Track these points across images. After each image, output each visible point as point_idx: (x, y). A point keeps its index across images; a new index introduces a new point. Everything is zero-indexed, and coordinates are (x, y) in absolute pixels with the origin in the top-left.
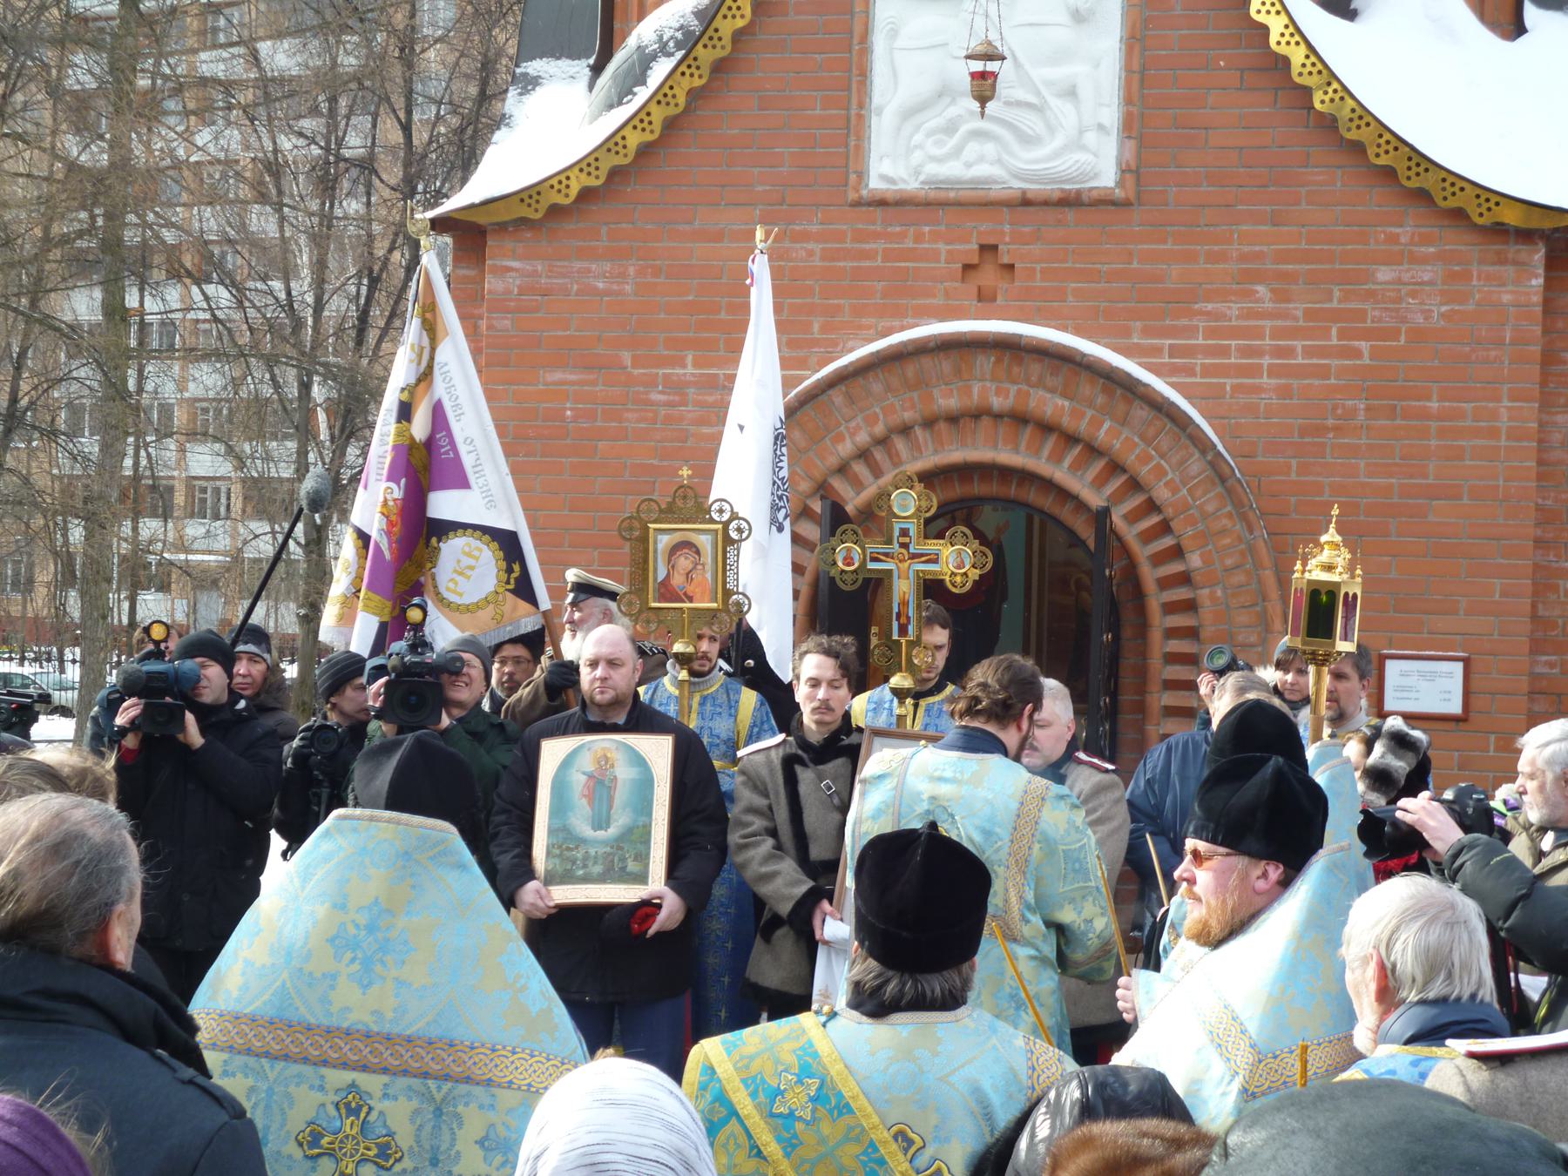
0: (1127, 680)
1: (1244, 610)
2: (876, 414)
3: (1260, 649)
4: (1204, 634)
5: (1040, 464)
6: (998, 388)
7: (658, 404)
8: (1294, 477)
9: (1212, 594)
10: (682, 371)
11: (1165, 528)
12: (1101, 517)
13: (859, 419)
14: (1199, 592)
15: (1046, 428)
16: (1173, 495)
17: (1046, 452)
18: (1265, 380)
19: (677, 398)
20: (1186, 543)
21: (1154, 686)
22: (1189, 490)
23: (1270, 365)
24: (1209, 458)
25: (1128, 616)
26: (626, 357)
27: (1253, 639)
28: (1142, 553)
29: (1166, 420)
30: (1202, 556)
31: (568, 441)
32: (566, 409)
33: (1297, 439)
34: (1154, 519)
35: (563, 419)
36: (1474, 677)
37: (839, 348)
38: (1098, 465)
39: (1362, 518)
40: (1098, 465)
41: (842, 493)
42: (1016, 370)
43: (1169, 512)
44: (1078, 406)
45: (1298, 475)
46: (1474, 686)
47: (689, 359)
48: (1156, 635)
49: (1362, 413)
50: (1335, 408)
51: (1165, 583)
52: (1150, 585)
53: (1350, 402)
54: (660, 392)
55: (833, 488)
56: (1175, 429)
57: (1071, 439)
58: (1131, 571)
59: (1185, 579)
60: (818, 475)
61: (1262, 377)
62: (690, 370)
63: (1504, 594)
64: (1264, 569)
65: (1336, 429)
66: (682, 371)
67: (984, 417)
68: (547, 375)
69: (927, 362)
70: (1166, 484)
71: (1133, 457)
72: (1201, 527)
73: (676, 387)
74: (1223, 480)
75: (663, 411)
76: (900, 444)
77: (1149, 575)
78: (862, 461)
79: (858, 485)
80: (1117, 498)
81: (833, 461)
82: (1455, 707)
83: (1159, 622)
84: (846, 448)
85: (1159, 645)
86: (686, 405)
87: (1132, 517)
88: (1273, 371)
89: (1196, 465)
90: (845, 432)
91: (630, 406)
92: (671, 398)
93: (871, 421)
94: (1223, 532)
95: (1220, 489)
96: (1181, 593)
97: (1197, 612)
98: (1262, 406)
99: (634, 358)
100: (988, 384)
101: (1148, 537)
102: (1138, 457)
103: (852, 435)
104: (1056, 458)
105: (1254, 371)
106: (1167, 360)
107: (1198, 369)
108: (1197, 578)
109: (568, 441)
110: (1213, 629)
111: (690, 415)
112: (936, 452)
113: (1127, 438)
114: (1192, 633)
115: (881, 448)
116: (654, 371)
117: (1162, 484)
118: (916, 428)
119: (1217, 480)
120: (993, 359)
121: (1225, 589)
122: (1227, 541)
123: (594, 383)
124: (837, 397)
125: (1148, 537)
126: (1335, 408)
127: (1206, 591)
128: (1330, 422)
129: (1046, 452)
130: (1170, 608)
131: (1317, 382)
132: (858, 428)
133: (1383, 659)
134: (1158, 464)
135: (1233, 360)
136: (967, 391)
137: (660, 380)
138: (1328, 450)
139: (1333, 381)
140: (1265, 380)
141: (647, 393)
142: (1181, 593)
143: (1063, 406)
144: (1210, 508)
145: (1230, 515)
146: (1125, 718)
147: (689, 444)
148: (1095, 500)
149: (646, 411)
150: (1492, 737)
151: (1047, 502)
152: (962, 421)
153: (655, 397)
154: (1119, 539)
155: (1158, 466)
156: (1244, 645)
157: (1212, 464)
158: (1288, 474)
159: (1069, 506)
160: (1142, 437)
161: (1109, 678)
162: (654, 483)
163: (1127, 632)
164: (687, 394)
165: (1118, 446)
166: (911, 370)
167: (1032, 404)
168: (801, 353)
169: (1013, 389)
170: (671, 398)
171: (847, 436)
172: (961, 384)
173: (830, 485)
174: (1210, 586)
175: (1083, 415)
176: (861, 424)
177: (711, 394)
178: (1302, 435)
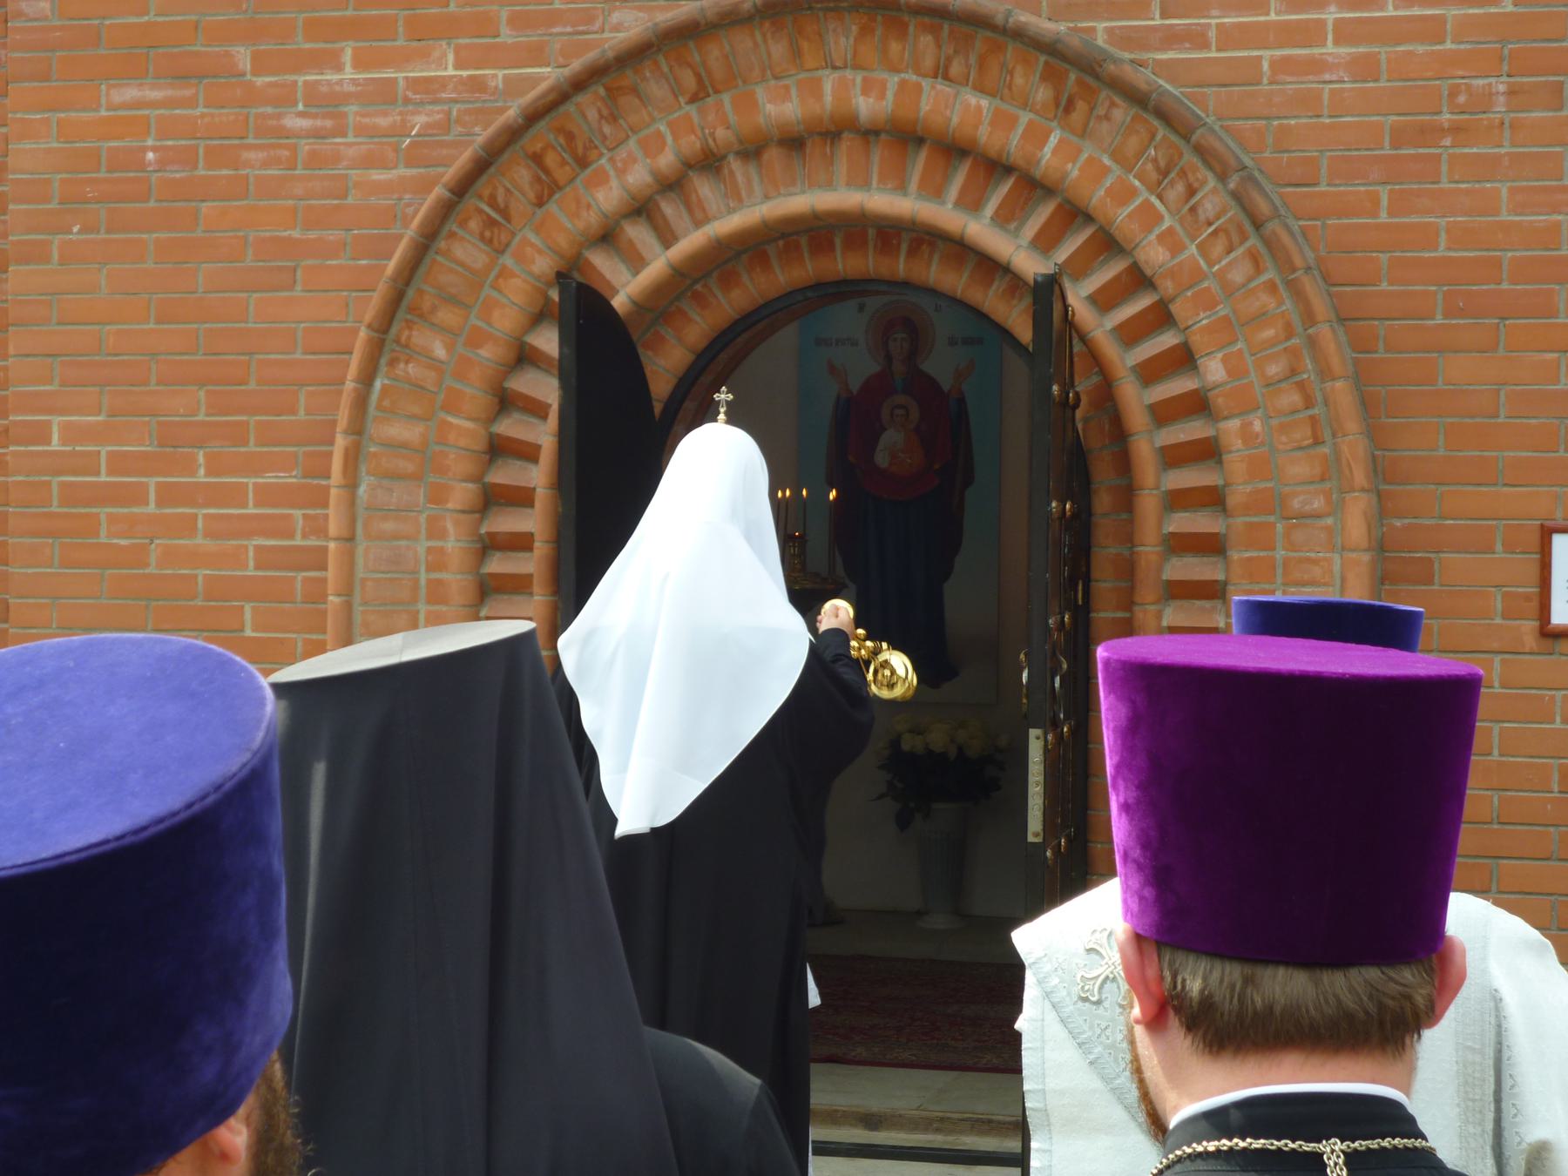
0: (1104, 583)
1: (1299, 454)
2: (659, 135)
3: (1329, 521)
4: (1232, 500)
5: (945, 214)
6: (865, 79)
7: (299, 134)
8: (1383, 217)
9: (1246, 428)
10: (335, 77)
11: (1161, 317)
12: (1046, 292)
13: (632, 144)
14: (1223, 425)
15: (953, 150)
16: (1173, 256)
17: (953, 191)
18: (1330, 48)
19: (328, 123)
20: (1197, 341)
21: (1147, 593)
22: (1199, 247)
23: (1337, 22)
24: (1232, 186)
25: (1103, 477)
26: (243, 56)
27: (1318, 504)
28: (1124, 361)
29: (1156, 123)
30: (1225, 360)
31: (152, 204)
32: (144, 150)
33: (1388, 151)
34: (1142, 302)
35: (142, 166)
37: (597, 25)
38: (1043, 213)
39: (1505, 286)
40: (1043, 213)
41: (608, 276)
42: (895, 47)
43: (1168, 286)
44: (1005, 107)
45: (1391, 214)
47: (347, 56)
48: (1148, 503)
49: (1502, 99)
50: (1454, 93)
51: (1164, 414)
53: (1481, 82)
54: (301, 115)
55: (594, 268)
56: (1173, 138)
57: (994, 167)
58: (1106, 395)
59: (1197, 404)
60: (563, 242)
61: (1324, 45)
62: (349, 73)
65: (1456, 129)
66: (335, 77)
67: (845, 135)
68: (113, 92)
69: (742, 42)
70: (1160, 238)
71: (1102, 192)
72: (1223, 310)
73: (326, 102)
74: (1258, 225)
75: (305, 146)
76: (704, 189)
77: (1135, 399)
78: (642, 220)
79: (636, 262)
80: (1079, 266)
81: (591, 220)
83: (1155, 481)
84: (608, 197)
86: (344, 135)
87: (1104, 301)
88: (1344, 33)
89: (1212, 199)
90: (608, 167)
91: (250, 141)
92: (319, 123)
93: (652, 146)
94: (1260, 319)
95: (1253, 241)
96: (1190, 430)
97: (1220, 462)
98: (1326, 96)
99: (256, 57)
100: (849, 73)
101: (1131, 334)
102: (1109, 191)
103: (621, 172)
104: (971, 202)
105: (1310, 35)
106: (1158, 22)
107: (1212, 34)
108: (1219, 401)
109: (152, 204)
110: (1249, 488)
111: (351, 152)
112: (767, 197)
113: (1091, 160)
114: (1213, 499)
115: (673, 195)
116: (290, 78)
117: (1153, 237)
118: (731, 158)
119: (1248, 227)
120: (854, 28)
122: (1269, 333)
123: (191, 103)
124: (588, 106)
125: (1131, 334)
126: (1454, 93)
127: (1234, 424)
128: (1446, 117)
129: (953, 191)
130: (1174, 457)
131: (1421, 49)
132: (632, 159)
134: (1147, 203)
135: (1273, 17)
136: (814, 88)
137: (299, 95)
138: (1444, 168)
139: (1449, 45)
140: (1330, 48)
141: (279, 116)
142: (1190, 430)
143: (979, 108)
144: (1237, 276)
145: (1272, 287)
147: (350, 200)
148: (1031, 265)
149: (280, 146)
151: (956, 282)
152: (809, 144)
153: (293, 122)
154: (1083, 338)
155: (1147, 206)
157: (1236, 196)
158: (1375, 215)
159: (999, 285)
160: (1116, 156)
161: (1072, 582)
163: (1103, 502)
164: (344, 115)
165: (1075, 173)
166: (714, 54)
167: (925, 106)
168: (533, 37)
169: (893, 81)
170: (319, 123)
171: (612, 173)
172: (803, 75)
173: (588, 263)
174: (1240, 414)
175: (1014, 121)
176: (639, 154)
177: (385, 114)
178: (1395, 145)
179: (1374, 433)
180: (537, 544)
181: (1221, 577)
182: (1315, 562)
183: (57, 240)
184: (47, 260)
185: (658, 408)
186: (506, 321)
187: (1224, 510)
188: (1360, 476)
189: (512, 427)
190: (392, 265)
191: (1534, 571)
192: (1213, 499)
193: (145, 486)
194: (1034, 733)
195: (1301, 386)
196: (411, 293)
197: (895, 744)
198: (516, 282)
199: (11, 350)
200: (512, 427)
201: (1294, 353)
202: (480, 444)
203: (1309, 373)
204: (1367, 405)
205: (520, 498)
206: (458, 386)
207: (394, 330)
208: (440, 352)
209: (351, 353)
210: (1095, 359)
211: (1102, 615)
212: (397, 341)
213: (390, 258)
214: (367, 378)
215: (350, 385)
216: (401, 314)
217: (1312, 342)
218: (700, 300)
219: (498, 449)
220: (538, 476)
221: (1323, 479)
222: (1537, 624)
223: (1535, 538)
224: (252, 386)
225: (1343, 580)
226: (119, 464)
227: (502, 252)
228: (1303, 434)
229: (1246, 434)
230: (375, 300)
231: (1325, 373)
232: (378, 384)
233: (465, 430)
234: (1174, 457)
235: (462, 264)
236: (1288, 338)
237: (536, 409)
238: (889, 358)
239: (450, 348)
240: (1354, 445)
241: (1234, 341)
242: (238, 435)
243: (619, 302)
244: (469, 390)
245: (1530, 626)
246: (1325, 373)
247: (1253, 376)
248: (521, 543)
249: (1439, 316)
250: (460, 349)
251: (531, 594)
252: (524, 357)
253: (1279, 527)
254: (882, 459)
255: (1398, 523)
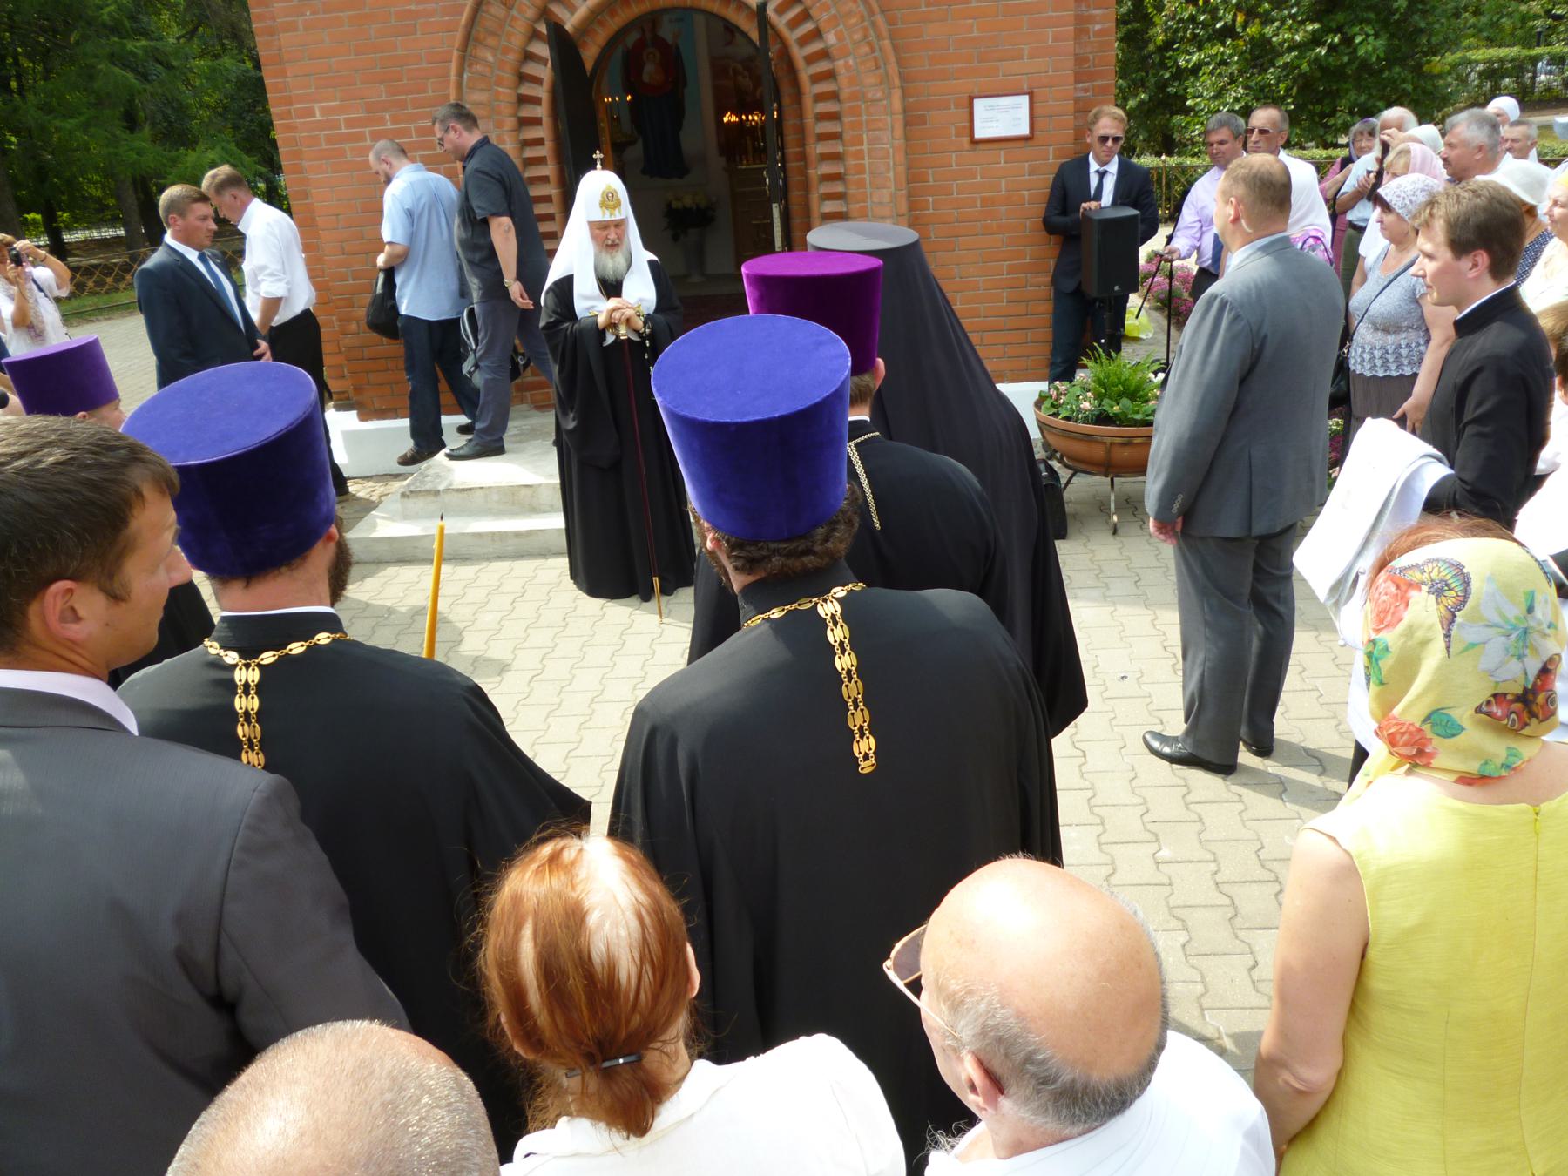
0: (790, 137)
3: (885, 102)
4: (844, 94)
9: (847, 63)
20: (822, 25)
21: (811, 140)
25: (786, 90)
27: (879, 95)
28: (792, 37)
30: (835, 34)
36: (1036, 105)
41: (560, 16)
46: (1037, 110)
48: (808, 100)
51: (810, 60)
52: (800, 63)
55: (554, 14)
58: (785, 52)
59: (824, 54)
63: (1055, 39)
64: (883, 39)
72: (833, 11)
77: (799, 54)
82: (1024, 130)
83: (810, 90)
85: (812, 108)
94: (850, 14)
96: (822, 66)
101: (794, 24)
108: (834, 52)
114: (834, 96)
121: (855, 58)
122: (854, 20)
125: (794, 24)
127: (840, 63)
130: (816, 79)
133: (971, 99)
142: (822, 66)
146: (793, 165)
150: (1051, 149)
154: (773, 28)
156: (872, 101)
162: (415, 24)
173: (551, 11)
179: (900, 61)
180: (546, 143)
181: (839, 130)
182: (880, 120)
183: (301, 19)
184: (296, 29)
185: (588, 74)
186: (517, 41)
187: (839, 101)
188: (897, 82)
189: (528, 90)
190: (464, 19)
191: (967, 116)
192: (834, 96)
193: (364, 132)
194: (774, 205)
195: (870, 44)
196: (474, 32)
197: (669, 205)
198: (519, 23)
199: (289, 74)
200: (528, 90)
201: (865, 29)
202: (514, 99)
203: (872, 38)
204: (895, 48)
205: (536, 122)
206: (501, 74)
207: (469, 49)
208: (490, 58)
209: (451, 61)
210: (779, 37)
211: (791, 150)
212: (471, 55)
213: (461, 14)
214: (460, 74)
215: (453, 77)
216: (471, 43)
217: (874, 24)
218: (601, 23)
219: (523, 100)
220: (542, 111)
221: (881, 84)
222: (968, 138)
223: (967, 101)
224: (405, 82)
225: (893, 127)
226: (350, 123)
227: (511, 8)
228: (871, 64)
229: (847, 66)
230: (459, 36)
231: (879, 37)
232: (465, 76)
233: (506, 93)
234: (816, 79)
235: (494, 16)
236: (862, 22)
237: (537, 81)
238: (643, 31)
239: (494, 55)
240: (893, 68)
241: (839, 25)
242: (402, 105)
243: (568, 27)
244: (506, 75)
245: (966, 140)
246: (879, 37)
247: (848, 40)
248: (539, 142)
249: (923, 6)
250: (499, 56)
251: (546, 164)
252: (528, 57)
253: (863, 106)
254: (646, 78)
255: (911, 100)
